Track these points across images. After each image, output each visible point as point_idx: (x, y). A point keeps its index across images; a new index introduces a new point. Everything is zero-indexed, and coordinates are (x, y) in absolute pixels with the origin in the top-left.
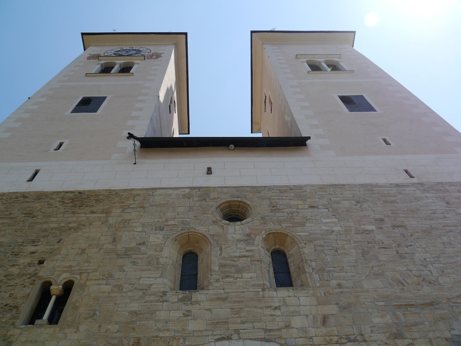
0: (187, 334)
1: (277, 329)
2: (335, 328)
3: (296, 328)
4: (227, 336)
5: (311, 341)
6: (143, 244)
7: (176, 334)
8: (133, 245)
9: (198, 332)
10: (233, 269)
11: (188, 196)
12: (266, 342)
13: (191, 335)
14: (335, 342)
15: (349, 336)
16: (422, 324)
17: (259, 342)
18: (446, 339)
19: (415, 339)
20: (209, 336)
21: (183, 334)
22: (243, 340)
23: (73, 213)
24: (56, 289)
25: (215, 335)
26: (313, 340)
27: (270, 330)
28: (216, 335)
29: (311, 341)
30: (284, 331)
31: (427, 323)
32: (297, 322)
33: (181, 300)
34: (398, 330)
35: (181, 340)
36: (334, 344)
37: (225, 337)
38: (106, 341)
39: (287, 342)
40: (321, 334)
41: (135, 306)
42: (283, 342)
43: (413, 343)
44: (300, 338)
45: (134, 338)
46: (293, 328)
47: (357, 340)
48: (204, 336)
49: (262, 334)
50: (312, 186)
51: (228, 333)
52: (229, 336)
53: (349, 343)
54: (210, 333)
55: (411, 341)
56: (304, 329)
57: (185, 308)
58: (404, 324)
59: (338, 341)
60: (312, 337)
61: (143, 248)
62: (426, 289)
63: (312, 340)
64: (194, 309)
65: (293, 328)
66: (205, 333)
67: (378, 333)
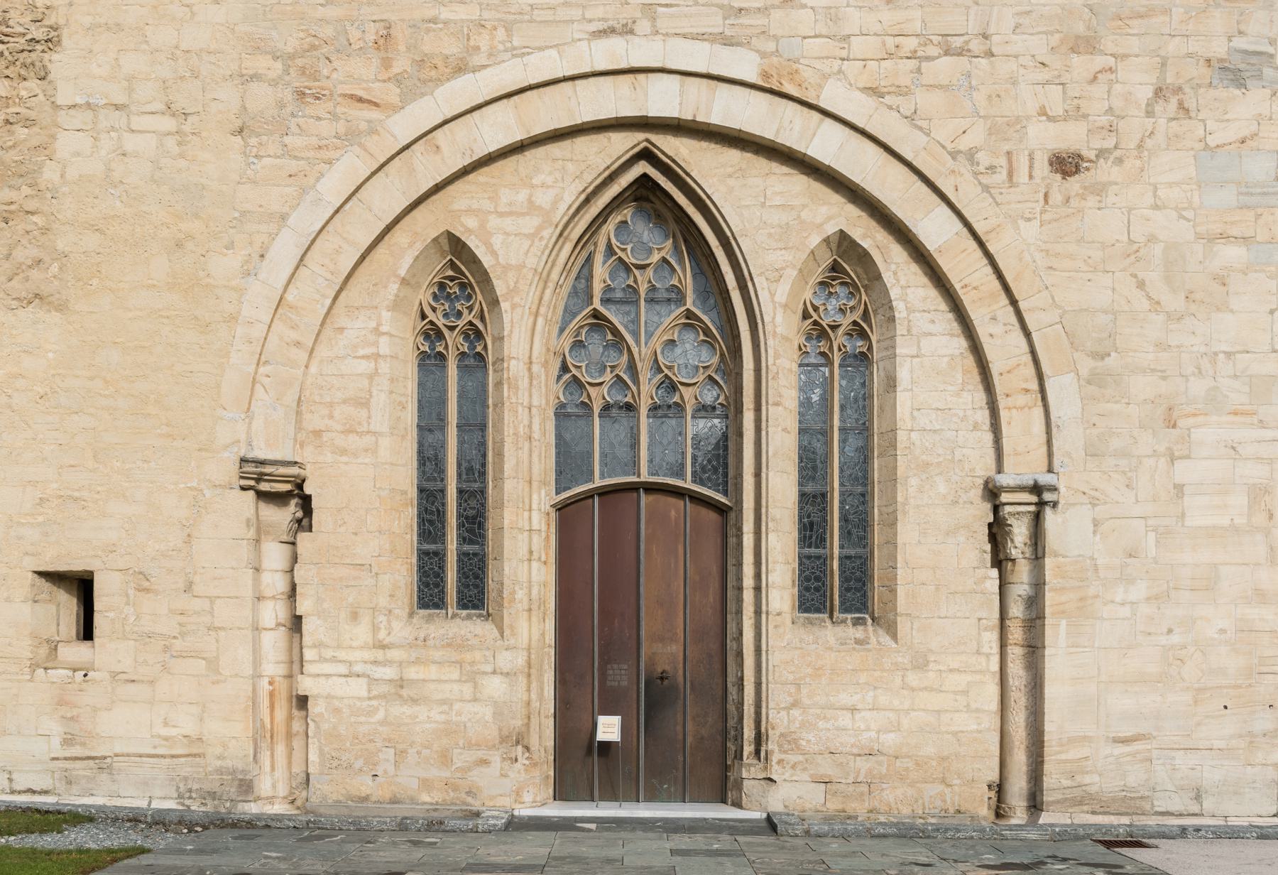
0: (515, 14)
1: (759, 9)
2: (917, 14)
3: (812, 8)
4: (623, 25)
5: (844, 48)
7: (486, 15)
9: (542, 9)
12: (725, 45)
13: (527, 17)
14: (909, 55)
15: (949, 38)
16: (1167, 11)
17: (706, 45)
18: (1209, 61)
19: (1125, 56)
20: (573, 22)
21: (505, 13)
22: (663, 38)
25: (590, 21)
26: (849, 46)
27: (741, 10)
28: (594, 20)
29: (844, 48)
30: (777, 15)
31: (1178, 12)
34: (1088, 28)
35: (501, 33)
36: (905, 60)
37: (617, 26)
38: (302, 31)
39: (780, 50)
40: (878, 28)
42: (771, 46)
43: (1114, 68)
44: (816, 36)
45: (374, 21)
46: (804, 6)
47: (969, 51)
48: (560, 21)
49: (715, 23)
51: (625, 15)
52: (627, 24)
53: (947, 58)
54: (576, 13)
55: (1111, 61)
56: (832, 11)
58: (1114, 10)
59: (916, 51)
60: (849, 36)
63: (846, 46)
65: (804, 6)
66: (563, 14)
67: (1032, 34)
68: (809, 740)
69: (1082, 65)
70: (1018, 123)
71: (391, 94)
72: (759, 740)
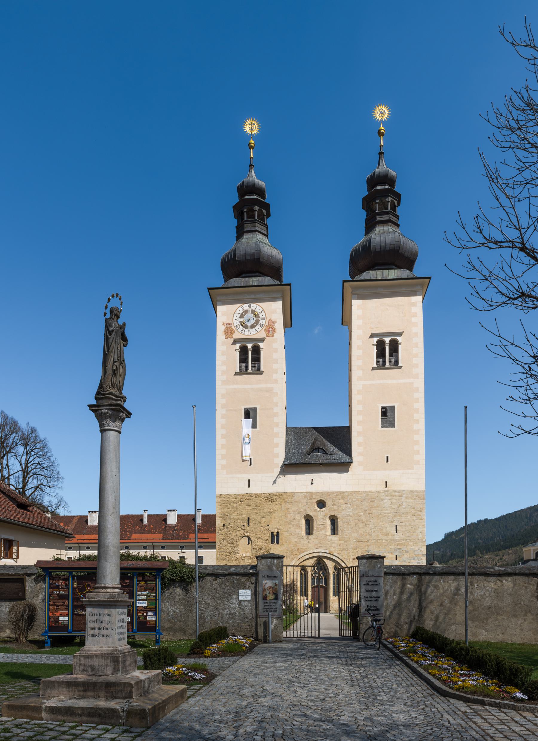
6: (294, 519)
8: (292, 520)
10: (319, 529)
11: (305, 497)
23: (270, 505)
24: (275, 534)
32: (334, 545)
33: (307, 538)
41: (296, 540)
49: (325, 548)
50: (348, 492)
57: (308, 540)
61: (295, 521)
62: (368, 537)
64: (310, 541)
68: (333, 607)
69: (355, 551)
70: (350, 556)
71: (299, 554)
72: (329, 607)
